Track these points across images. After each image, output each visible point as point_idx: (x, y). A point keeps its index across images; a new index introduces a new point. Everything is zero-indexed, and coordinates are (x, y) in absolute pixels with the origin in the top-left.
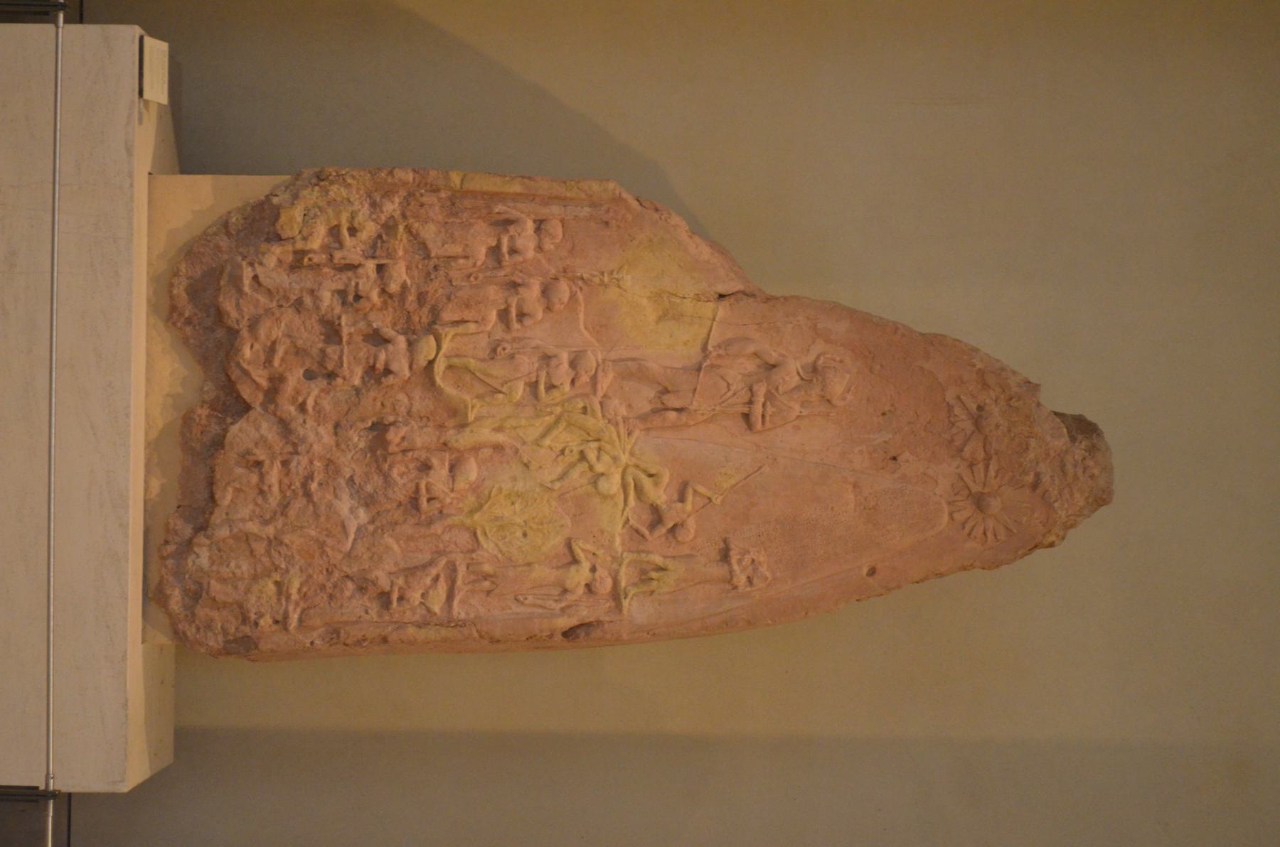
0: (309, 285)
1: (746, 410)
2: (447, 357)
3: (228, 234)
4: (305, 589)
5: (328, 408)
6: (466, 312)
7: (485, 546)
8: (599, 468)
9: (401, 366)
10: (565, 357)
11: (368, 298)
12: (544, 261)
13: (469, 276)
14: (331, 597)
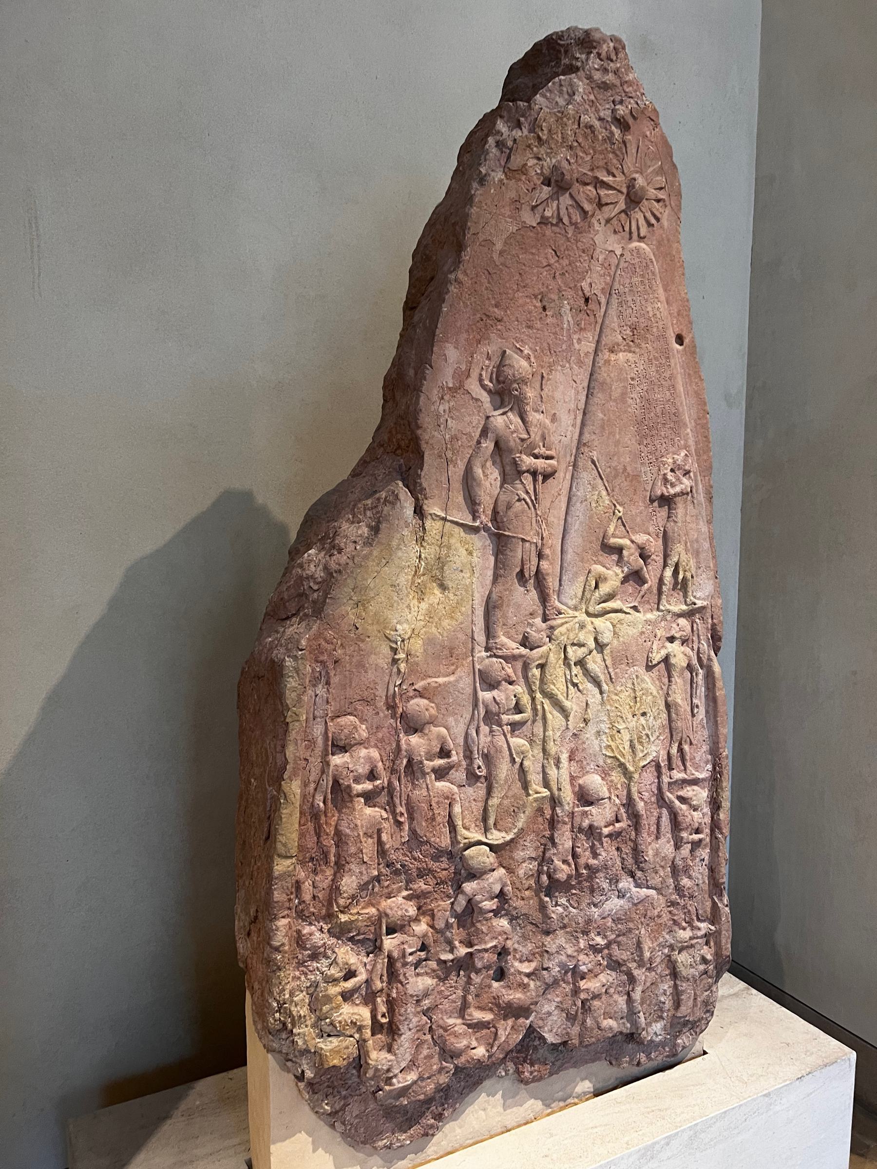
0: (411, 1009)
1: (540, 478)
2: (486, 830)
3: (343, 1109)
4: (684, 924)
5: (530, 946)
6: (439, 819)
7: (654, 754)
8: (592, 644)
9: (497, 878)
10: (485, 696)
11: (425, 935)
12: (380, 735)
13: (399, 824)
14: (691, 897)
